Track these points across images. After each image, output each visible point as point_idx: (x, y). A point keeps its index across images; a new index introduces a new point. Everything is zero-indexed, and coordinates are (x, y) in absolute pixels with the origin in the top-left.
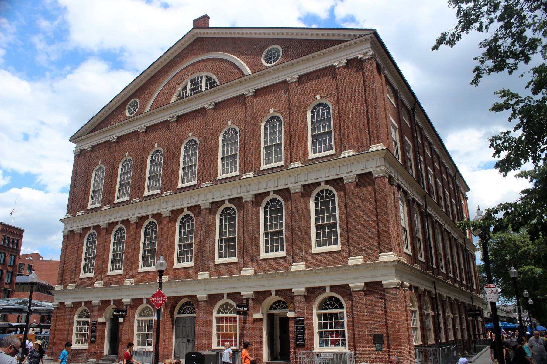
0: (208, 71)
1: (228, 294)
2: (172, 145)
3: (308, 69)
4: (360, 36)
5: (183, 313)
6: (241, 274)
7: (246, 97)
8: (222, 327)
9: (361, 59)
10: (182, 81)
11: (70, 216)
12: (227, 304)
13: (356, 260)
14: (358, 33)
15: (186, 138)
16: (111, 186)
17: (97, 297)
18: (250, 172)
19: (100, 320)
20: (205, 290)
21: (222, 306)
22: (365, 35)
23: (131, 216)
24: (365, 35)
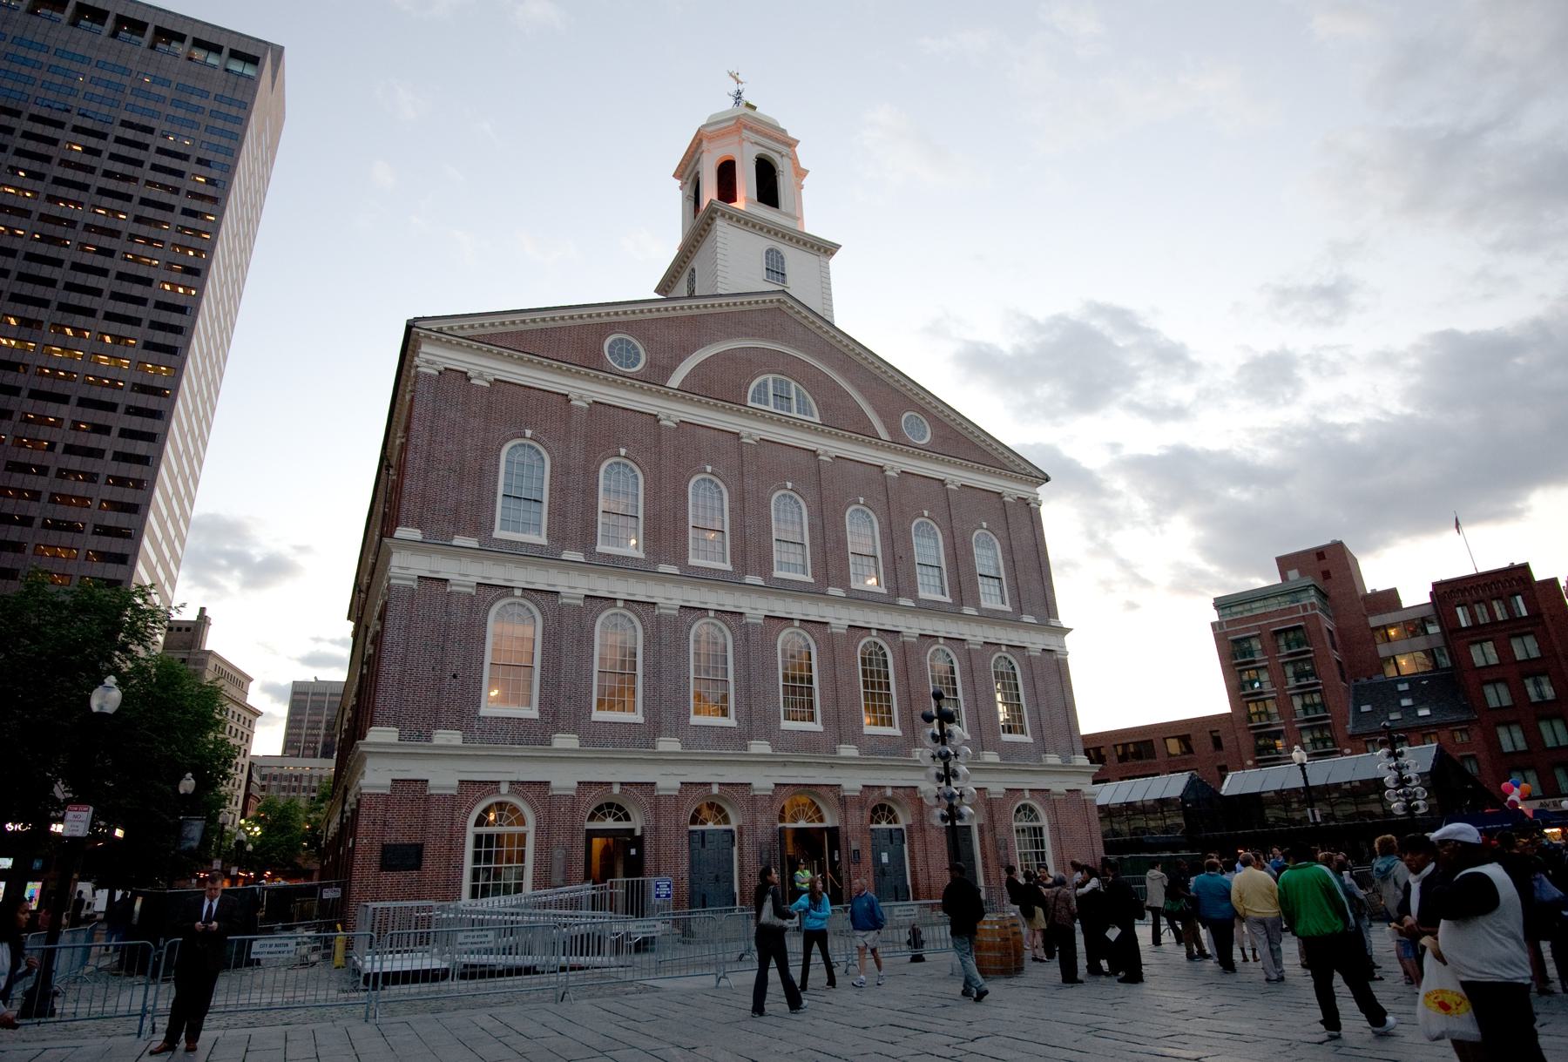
4: (1029, 475)
13: (1053, 759)
14: (1029, 469)
22: (1036, 477)
24: (1036, 477)
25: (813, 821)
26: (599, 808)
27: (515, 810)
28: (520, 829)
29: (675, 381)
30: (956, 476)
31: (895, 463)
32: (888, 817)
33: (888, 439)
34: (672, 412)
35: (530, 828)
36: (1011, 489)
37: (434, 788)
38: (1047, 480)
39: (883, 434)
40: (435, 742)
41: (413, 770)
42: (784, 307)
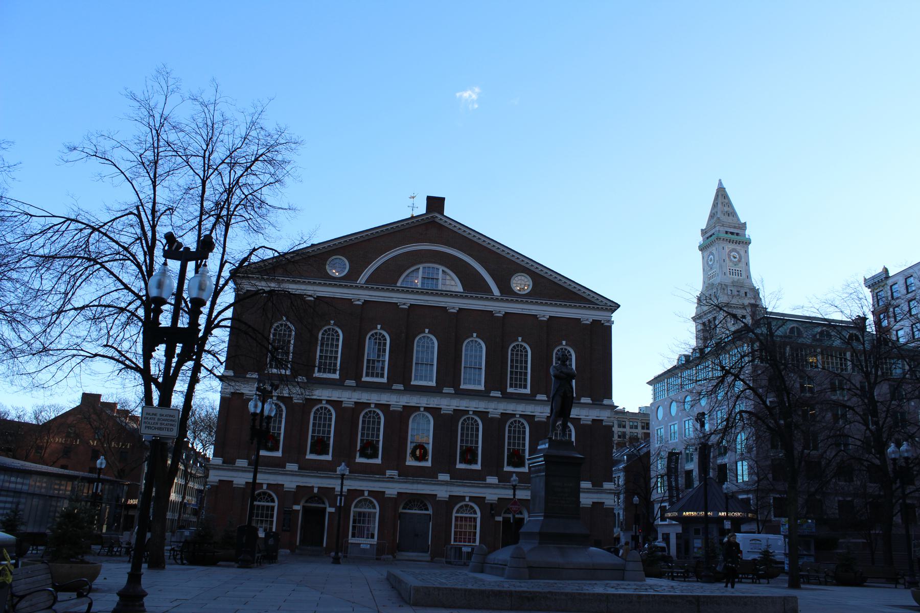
0: (448, 268)
5: (409, 509)
6: (485, 480)
8: (461, 526)
9: (603, 324)
11: (231, 373)
12: (467, 506)
14: (605, 301)
15: (419, 333)
17: (292, 481)
19: (296, 507)
20: (446, 491)
21: (461, 507)
22: (610, 306)
25: (422, 510)
27: (270, 496)
28: (271, 504)
29: (362, 279)
30: (545, 311)
31: (501, 308)
32: (469, 511)
33: (499, 294)
34: (359, 295)
35: (276, 504)
36: (587, 316)
37: (236, 484)
38: (619, 306)
39: (496, 292)
40: (236, 465)
41: (226, 476)
42: (437, 220)
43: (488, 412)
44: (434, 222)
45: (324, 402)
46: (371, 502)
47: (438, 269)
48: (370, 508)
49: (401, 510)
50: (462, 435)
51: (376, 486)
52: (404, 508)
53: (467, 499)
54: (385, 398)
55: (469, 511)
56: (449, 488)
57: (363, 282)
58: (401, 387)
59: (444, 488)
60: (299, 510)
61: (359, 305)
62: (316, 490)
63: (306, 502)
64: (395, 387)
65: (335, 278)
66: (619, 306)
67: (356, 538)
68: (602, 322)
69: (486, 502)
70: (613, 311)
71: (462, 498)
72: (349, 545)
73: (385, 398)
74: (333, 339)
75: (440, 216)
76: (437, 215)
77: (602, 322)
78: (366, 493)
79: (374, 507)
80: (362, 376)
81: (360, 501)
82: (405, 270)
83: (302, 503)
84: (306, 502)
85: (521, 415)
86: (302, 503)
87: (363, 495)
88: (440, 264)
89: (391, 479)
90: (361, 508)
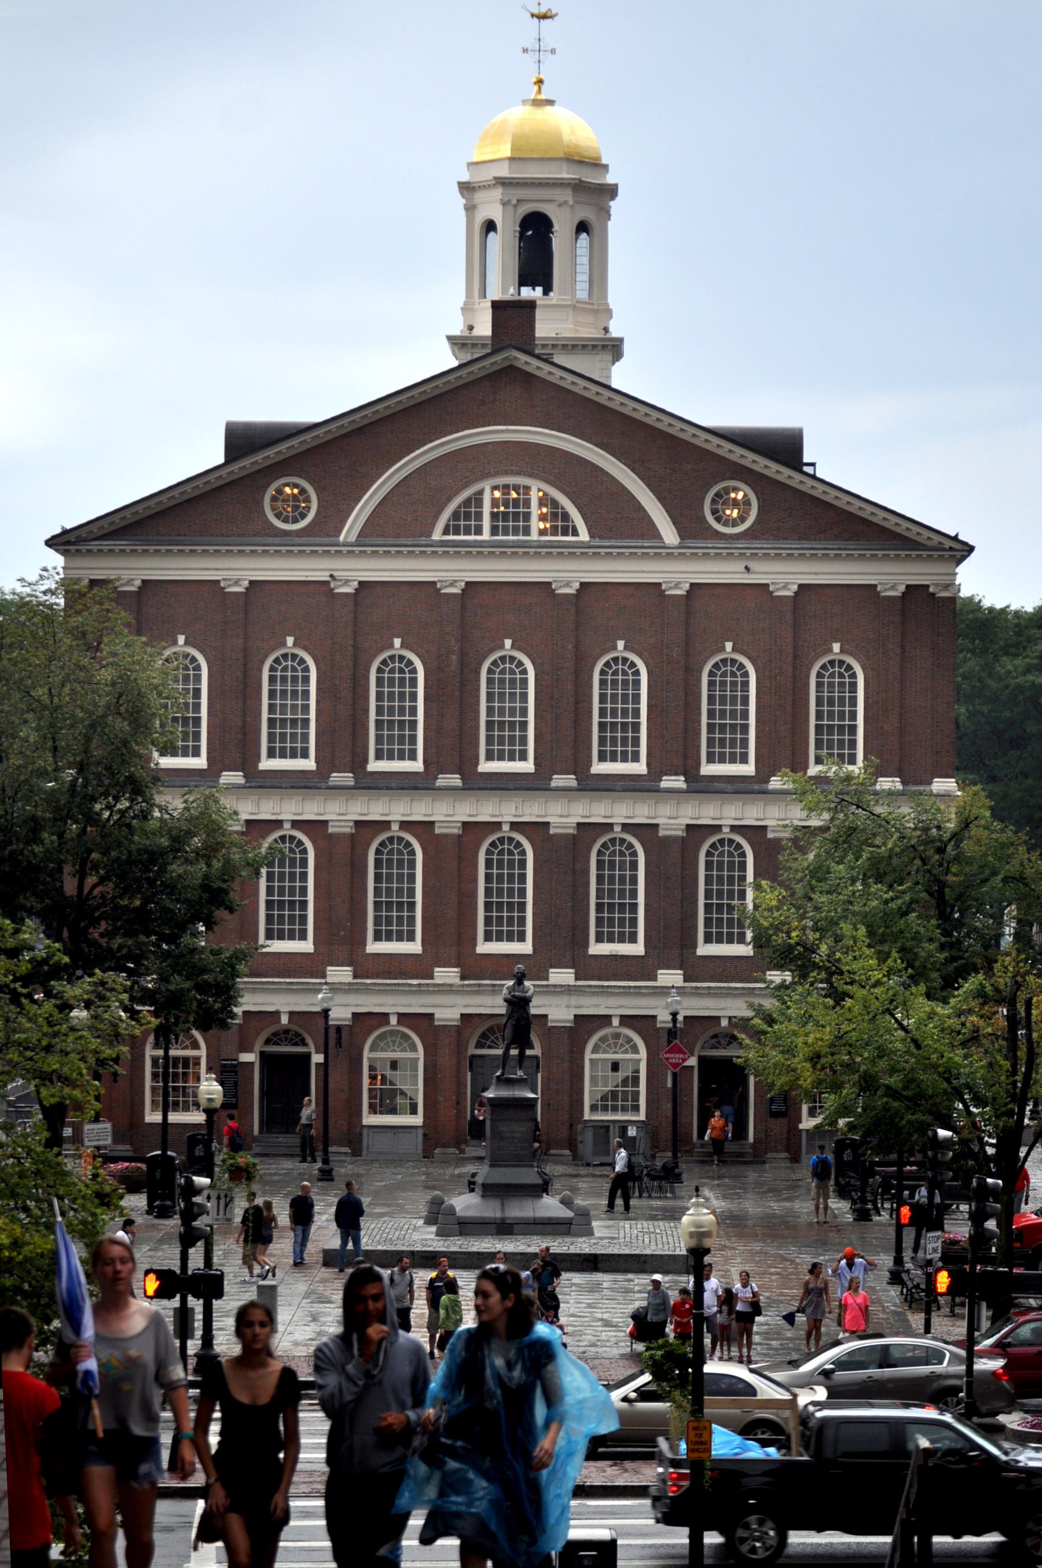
1: (622, 1016)
2: (454, 657)
3: (820, 577)
7: (665, 596)
9: (933, 594)
10: (466, 485)
14: (937, 538)
15: (492, 650)
16: (244, 721)
18: (676, 774)
20: (568, 1006)
21: (603, 1039)
23: (335, 817)
26: (275, 1034)
28: (189, 1053)
35: (202, 1053)
38: (971, 549)
39: (669, 535)
43: (657, 825)
44: (511, 367)
45: (287, 826)
46: (406, 1037)
47: (527, 489)
48: (404, 1050)
49: (472, 1051)
50: (600, 879)
51: (415, 1005)
52: (480, 1045)
53: (616, 1022)
54: (419, 809)
55: (622, 1045)
56: (574, 1000)
57: (352, 538)
58: (455, 780)
59: (563, 1000)
60: (253, 1063)
61: (347, 594)
62: (284, 1019)
63: (268, 1042)
64: (443, 780)
65: (286, 533)
66: (971, 549)
67: (378, 1116)
68: (931, 590)
69: (658, 1025)
70: (959, 561)
71: (606, 1020)
72: (365, 1132)
73: (419, 809)
74: (295, 679)
75: (523, 358)
76: (516, 354)
77: (931, 590)
78: (393, 1020)
79: (414, 1048)
80: (366, 761)
81: (381, 1037)
82: (449, 499)
83: (259, 1045)
84: (268, 1042)
85: (734, 828)
86: (259, 1045)
87: (388, 1023)
88: (531, 475)
89: (447, 989)
90: (383, 1050)
